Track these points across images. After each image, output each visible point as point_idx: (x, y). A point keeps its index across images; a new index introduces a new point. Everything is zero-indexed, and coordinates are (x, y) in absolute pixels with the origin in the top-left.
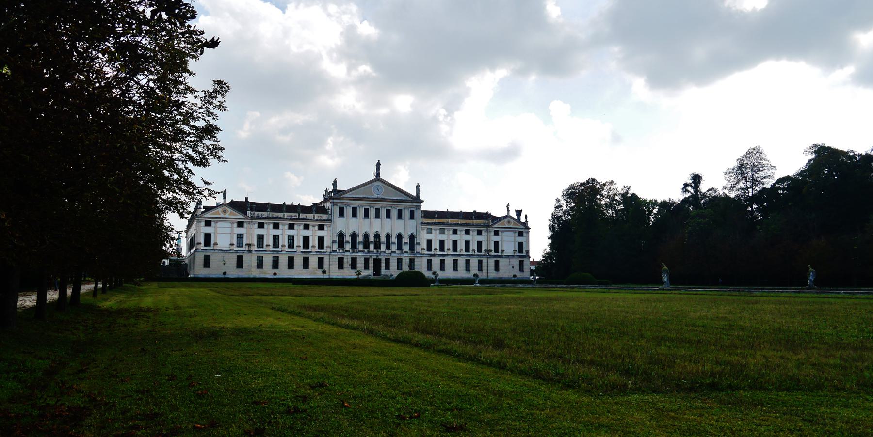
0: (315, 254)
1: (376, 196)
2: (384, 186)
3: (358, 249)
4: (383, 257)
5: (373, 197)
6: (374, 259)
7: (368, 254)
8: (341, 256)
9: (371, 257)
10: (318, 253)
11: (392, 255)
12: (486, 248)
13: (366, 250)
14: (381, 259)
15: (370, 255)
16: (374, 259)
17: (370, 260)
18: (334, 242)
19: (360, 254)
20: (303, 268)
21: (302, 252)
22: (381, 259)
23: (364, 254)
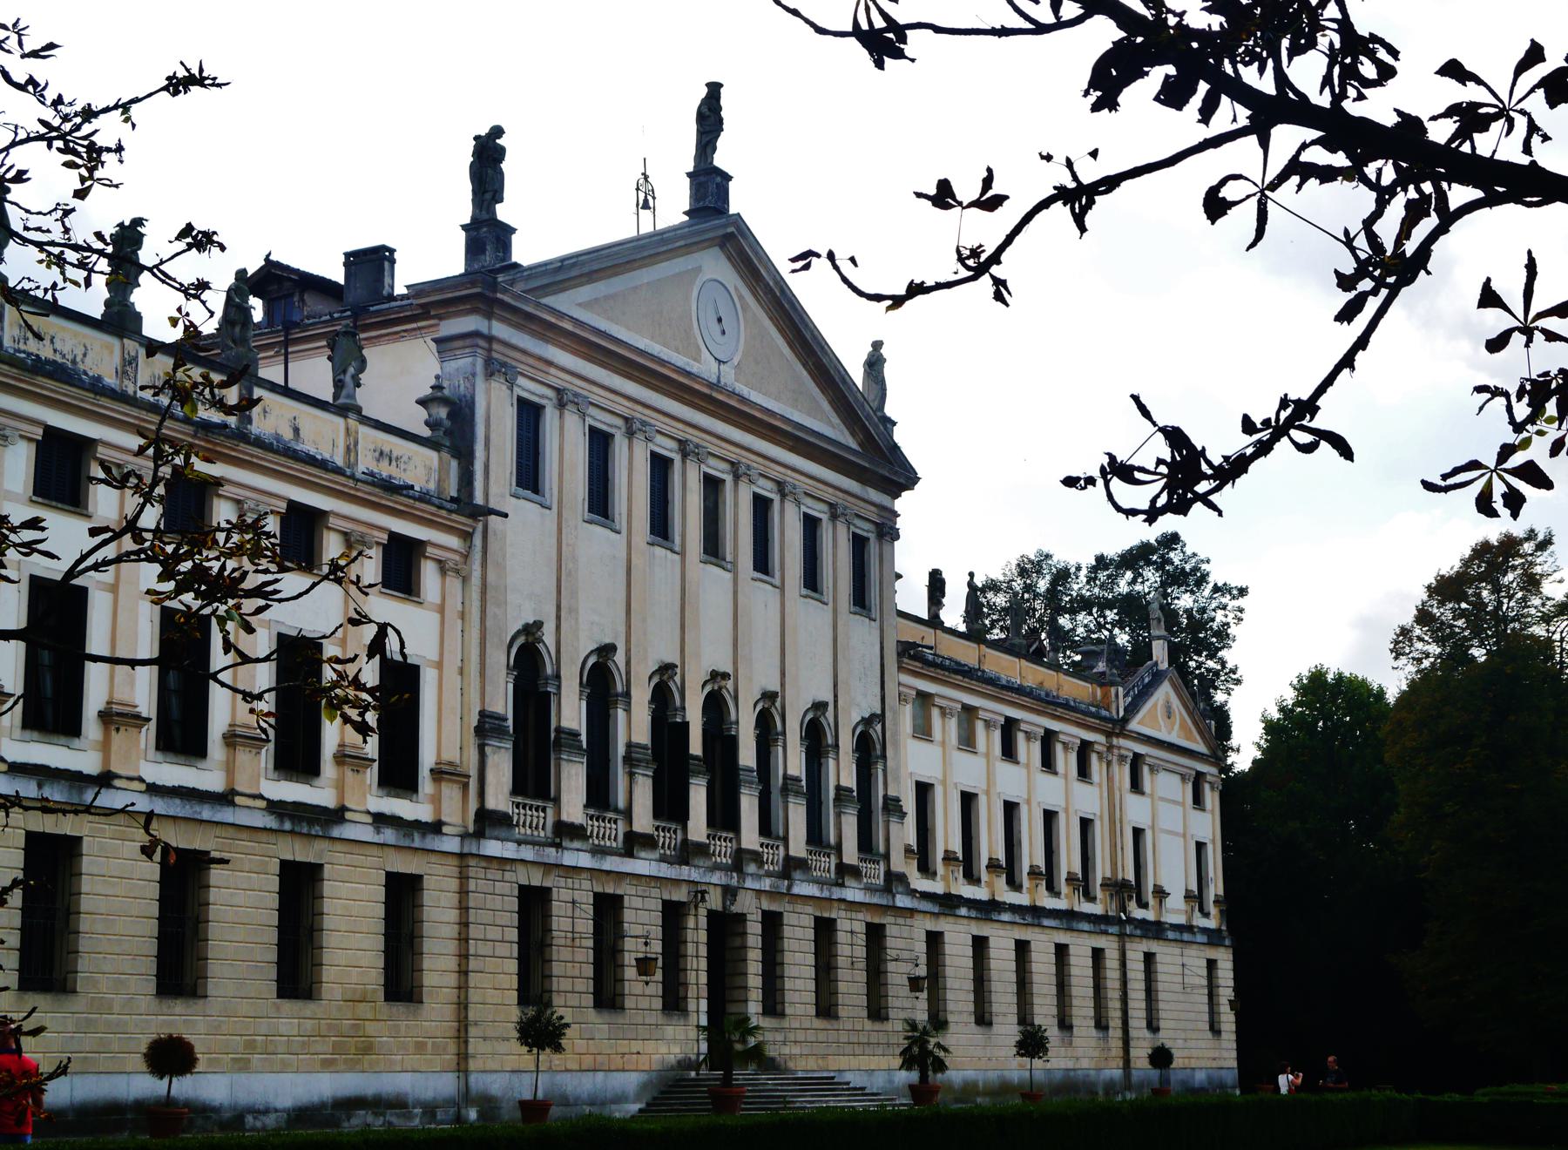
0: (366, 833)
1: (706, 368)
2: (745, 307)
3: (628, 814)
4: (749, 906)
5: (694, 368)
6: (711, 914)
7: (685, 872)
8: (536, 882)
9: (700, 894)
10: (389, 835)
11: (796, 890)
12: (1108, 875)
13: (669, 839)
14: (741, 918)
15: (695, 875)
16: (711, 914)
17: (691, 923)
18: (487, 727)
19: (643, 865)
20: (280, 996)
21: (276, 807)
22: (741, 918)
23: (665, 870)
